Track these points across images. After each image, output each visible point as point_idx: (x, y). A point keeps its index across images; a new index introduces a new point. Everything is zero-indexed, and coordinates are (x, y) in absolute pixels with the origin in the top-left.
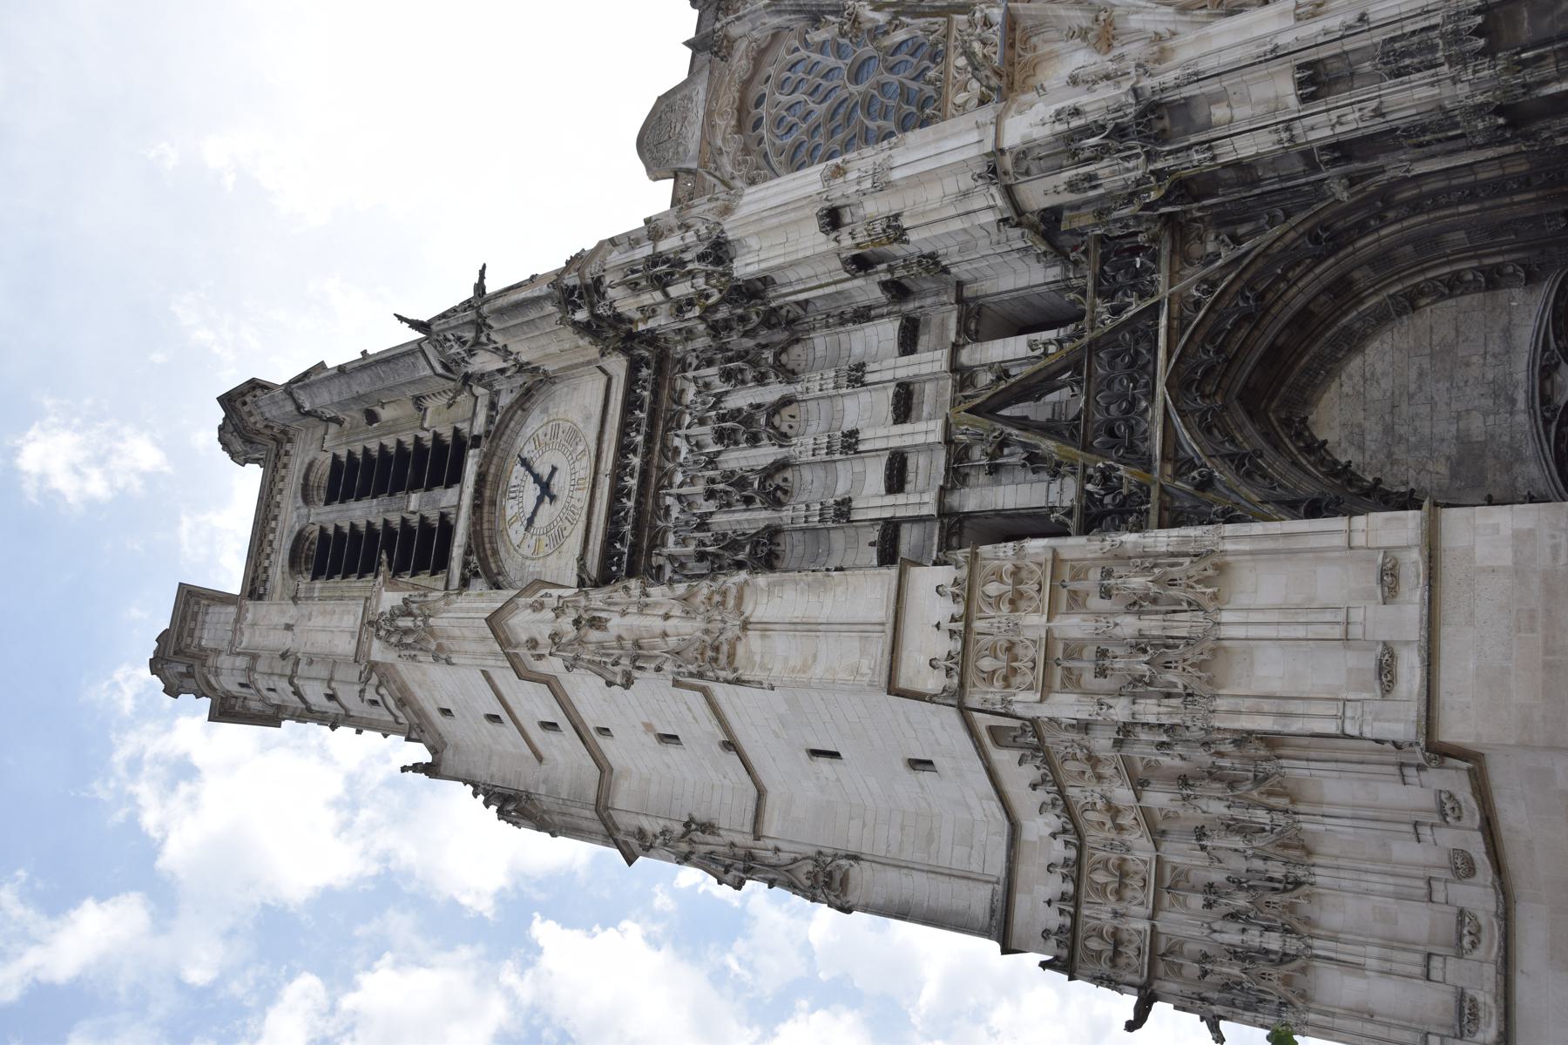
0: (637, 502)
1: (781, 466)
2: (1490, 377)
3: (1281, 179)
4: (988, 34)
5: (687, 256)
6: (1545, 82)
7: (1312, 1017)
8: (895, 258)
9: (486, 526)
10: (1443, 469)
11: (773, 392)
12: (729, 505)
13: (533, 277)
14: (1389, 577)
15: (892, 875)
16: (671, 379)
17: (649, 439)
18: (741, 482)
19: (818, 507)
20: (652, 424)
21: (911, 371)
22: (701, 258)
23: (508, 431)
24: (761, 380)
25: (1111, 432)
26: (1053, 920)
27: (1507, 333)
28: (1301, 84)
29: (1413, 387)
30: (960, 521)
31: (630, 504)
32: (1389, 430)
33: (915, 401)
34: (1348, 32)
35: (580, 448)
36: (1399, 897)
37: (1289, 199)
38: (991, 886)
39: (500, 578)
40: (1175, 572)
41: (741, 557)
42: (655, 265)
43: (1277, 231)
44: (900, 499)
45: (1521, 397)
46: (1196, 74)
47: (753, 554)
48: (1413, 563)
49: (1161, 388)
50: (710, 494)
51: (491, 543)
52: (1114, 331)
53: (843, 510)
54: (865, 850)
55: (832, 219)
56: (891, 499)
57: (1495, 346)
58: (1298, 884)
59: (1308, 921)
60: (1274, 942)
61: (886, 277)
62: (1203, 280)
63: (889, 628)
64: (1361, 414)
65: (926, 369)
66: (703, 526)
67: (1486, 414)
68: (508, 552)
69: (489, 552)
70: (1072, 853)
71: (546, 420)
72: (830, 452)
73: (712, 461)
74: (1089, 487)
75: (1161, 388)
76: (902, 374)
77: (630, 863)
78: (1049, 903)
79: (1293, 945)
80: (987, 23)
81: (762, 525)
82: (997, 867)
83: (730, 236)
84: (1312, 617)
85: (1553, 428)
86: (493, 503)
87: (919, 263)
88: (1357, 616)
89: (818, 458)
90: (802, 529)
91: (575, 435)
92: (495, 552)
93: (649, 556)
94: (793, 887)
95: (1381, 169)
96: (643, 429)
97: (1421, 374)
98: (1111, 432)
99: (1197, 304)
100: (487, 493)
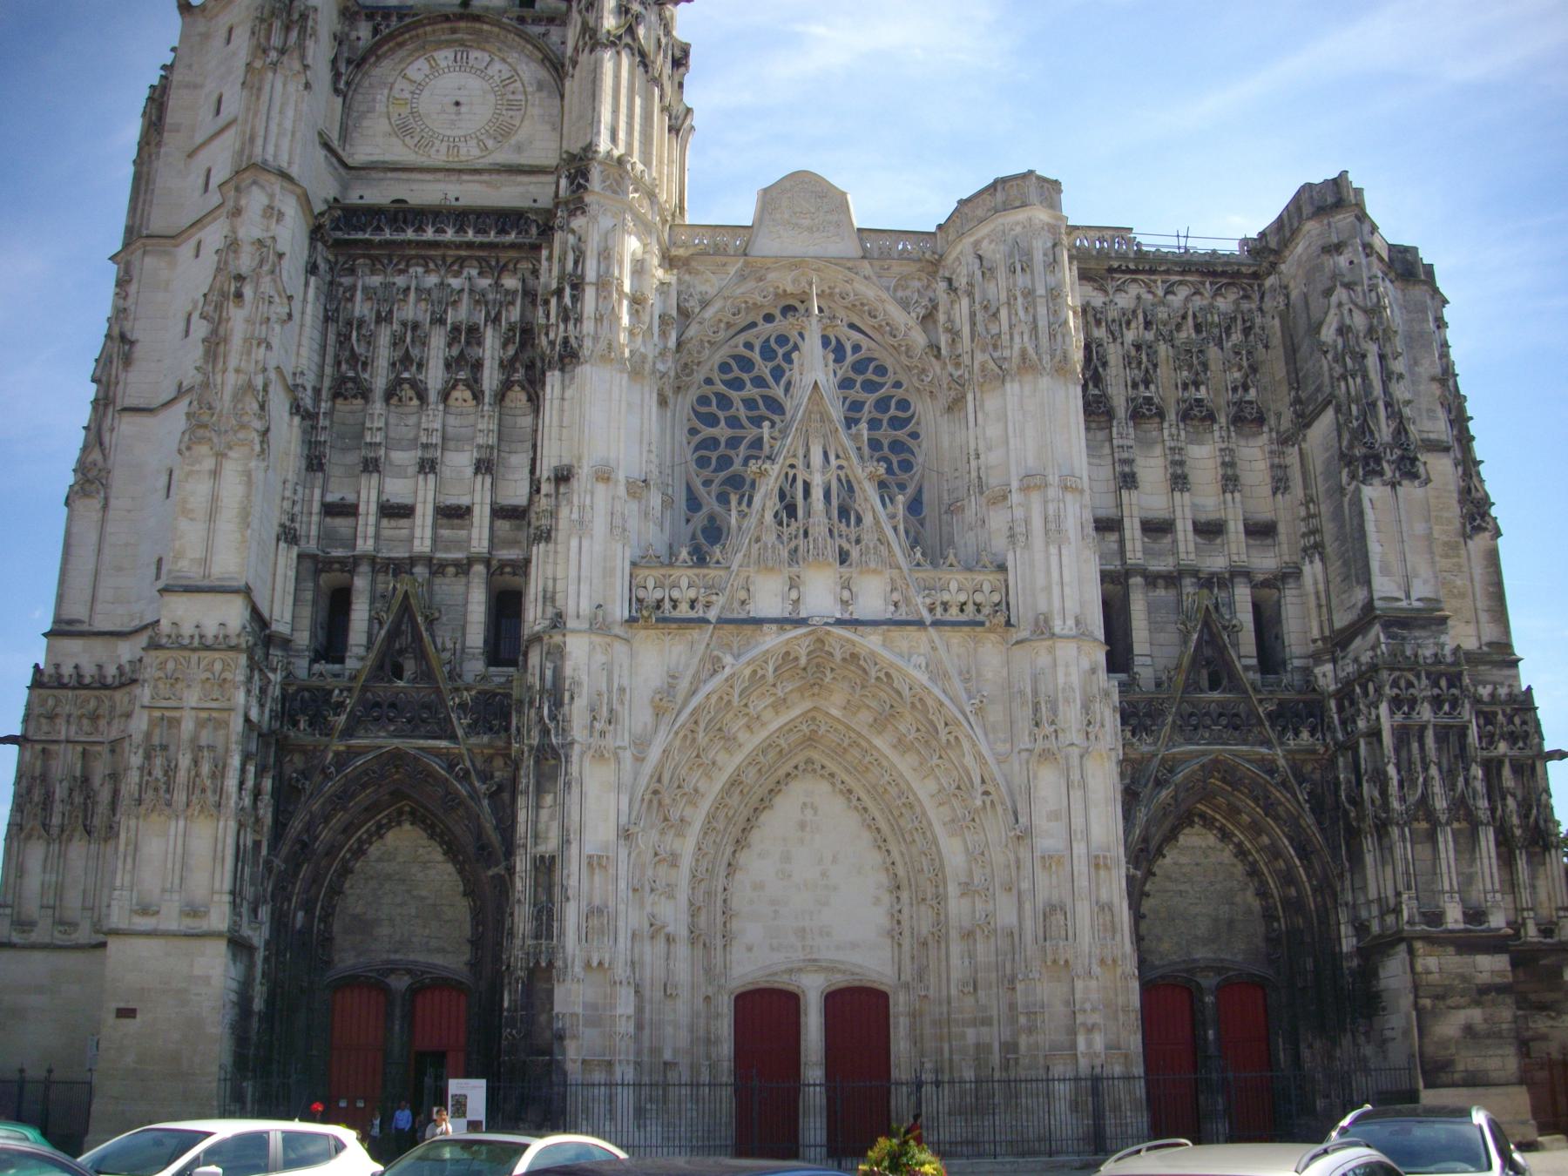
0: (410, 242)
1: (422, 396)
2: (414, 939)
5: (571, 326)
7: (16, 844)
9: (428, 29)
10: (358, 910)
11: (490, 378)
14: (193, 911)
15: (93, 537)
16: (527, 258)
17: (470, 245)
20: (482, 246)
21: (476, 520)
22: (566, 341)
23: (523, 42)
24: (501, 364)
26: (67, 670)
27: (442, 950)
28: (542, 857)
29: (415, 893)
30: (349, 571)
32: (389, 877)
33: (456, 521)
34: (564, 888)
35: (490, 143)
36: (84, 892)
38: (87, 620)
39: (373, 59)
40: (209, 793)
41: (344, 367)
42: (574, 287)
45: (398, 957)
46: (569, 788)
48: (204, 925)
49: (397, 742)
51: (411, 38)
52: (446, 707)
54: (111, 514)
55: (563, 477)
56: (373, 508)
57: (433, 943)
58: (89, 833)
59: (70, 839)
60: (56, 820)
63: (206, 583)
64: (401, 860)
65: (475, 533)
66: (379, 320)
67: (390, 936)
68: (401, 61)
69: (400, 39)
70: (109, 680)
71: (530, 89)
72: (425, 446)
73: (441, 321)
74: (337, 692)
75: (397, 742)
76: (476, 510)
77: (111, 259)
78: (76, 667)
79: (55, 831)
80: (708, 605)
82: (101, 624)
83: (578, 370)
84: (177, 873)
85: (374, 974)
86: (454, 31)
88: (176, 897)
89: (422, 433)
91: (503, 133)
92: (401, 45)
93: (364, 256)
94: (86, 449)
96: (480, 239)
97: (423, 899)
99: (451, 767)
100: (462, 24)
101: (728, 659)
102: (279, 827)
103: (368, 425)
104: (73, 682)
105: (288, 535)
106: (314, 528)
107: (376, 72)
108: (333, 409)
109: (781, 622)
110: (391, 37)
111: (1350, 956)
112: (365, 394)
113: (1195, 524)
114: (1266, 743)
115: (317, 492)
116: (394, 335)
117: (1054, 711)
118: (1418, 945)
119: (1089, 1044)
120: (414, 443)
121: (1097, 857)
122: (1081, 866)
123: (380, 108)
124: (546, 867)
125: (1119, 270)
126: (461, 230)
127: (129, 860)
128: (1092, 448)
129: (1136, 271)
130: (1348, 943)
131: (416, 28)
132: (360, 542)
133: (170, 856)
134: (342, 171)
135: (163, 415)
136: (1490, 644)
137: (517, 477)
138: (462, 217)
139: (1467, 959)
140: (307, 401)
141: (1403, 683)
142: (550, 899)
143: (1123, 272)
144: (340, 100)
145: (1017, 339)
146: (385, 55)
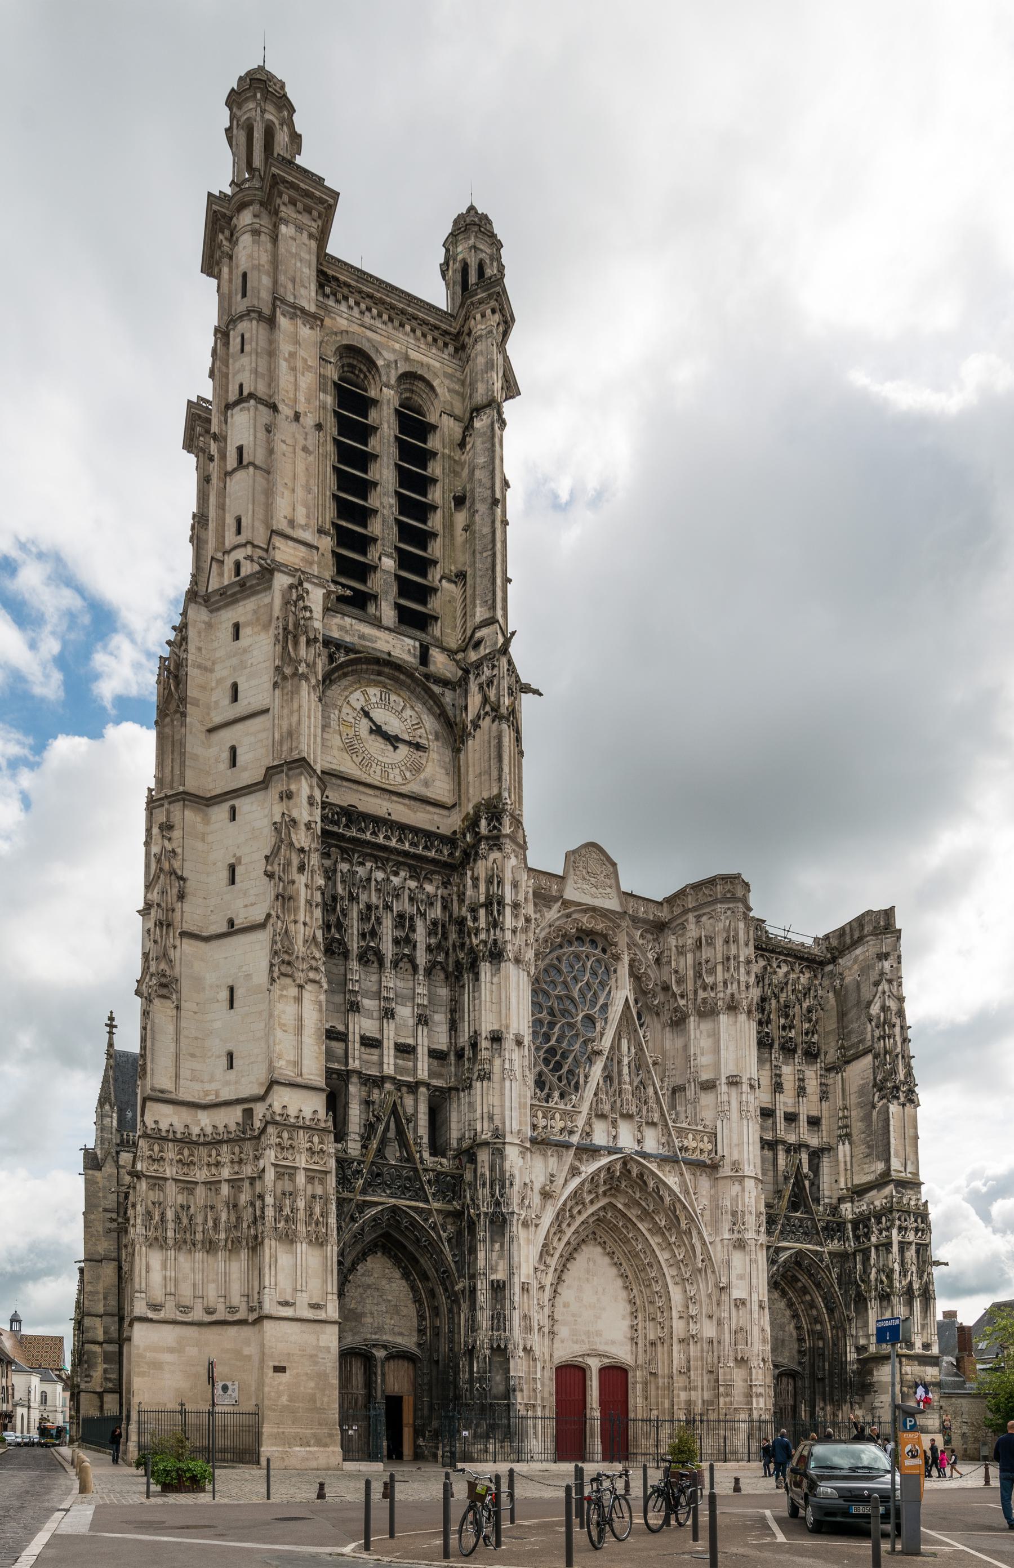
0: (369, 842)
3: (469, 1264)
4: (566, 1133)
6: (478, 1362)
8: (474, 1064)
9: (364, 667)
12: (362, 919)
13: (521, 753)
18: (373, 934)
19: (357, 989)
25: (378, 1175)
31: (368, 836)
37: (460, 1265)
41: (333, 930)
43: (450, 1258)
44: (357, 1045)
47: (333, 940)
50: (369, 907)
53: (354, 1007)
56: (357, 1038)
61: (466, 1053)
62: (435, 1224)
66: (353, 898)
68: (345, 689)
69: (346, 670)
80: (571, 1132)
81: (350, 948)
87: (468, 1078)
90: (345, 975)
93: (336, 846)
95: (464, 1302)
98: (378, 1175)
99: (426, 1220)
101: (583, 1168)
103: (349, 977)
104: (202, 1140)
109: (611, 1151)
110: (341, 666)
111: (852, 1363)
112: (346, 955)
116: (360, 912)
117: (743, 1217)
118: (904, 1359)
119: (758, 1404)
120: (378, 995)
121: (761, 1301)
122: (755, 1307)
124: (498, 1288)
126: (400, 840)
127: (273, 1268)
128: (761, 1061)
130: (852, 1356)
131: (356, 664)
133: (299, 1267)
135: (214, 944)
137: (438, 1029)
138: (403, 829)
139: (922, 1368)
141: (903, 1219)
142: (503, 1308)
145: (729, 985)
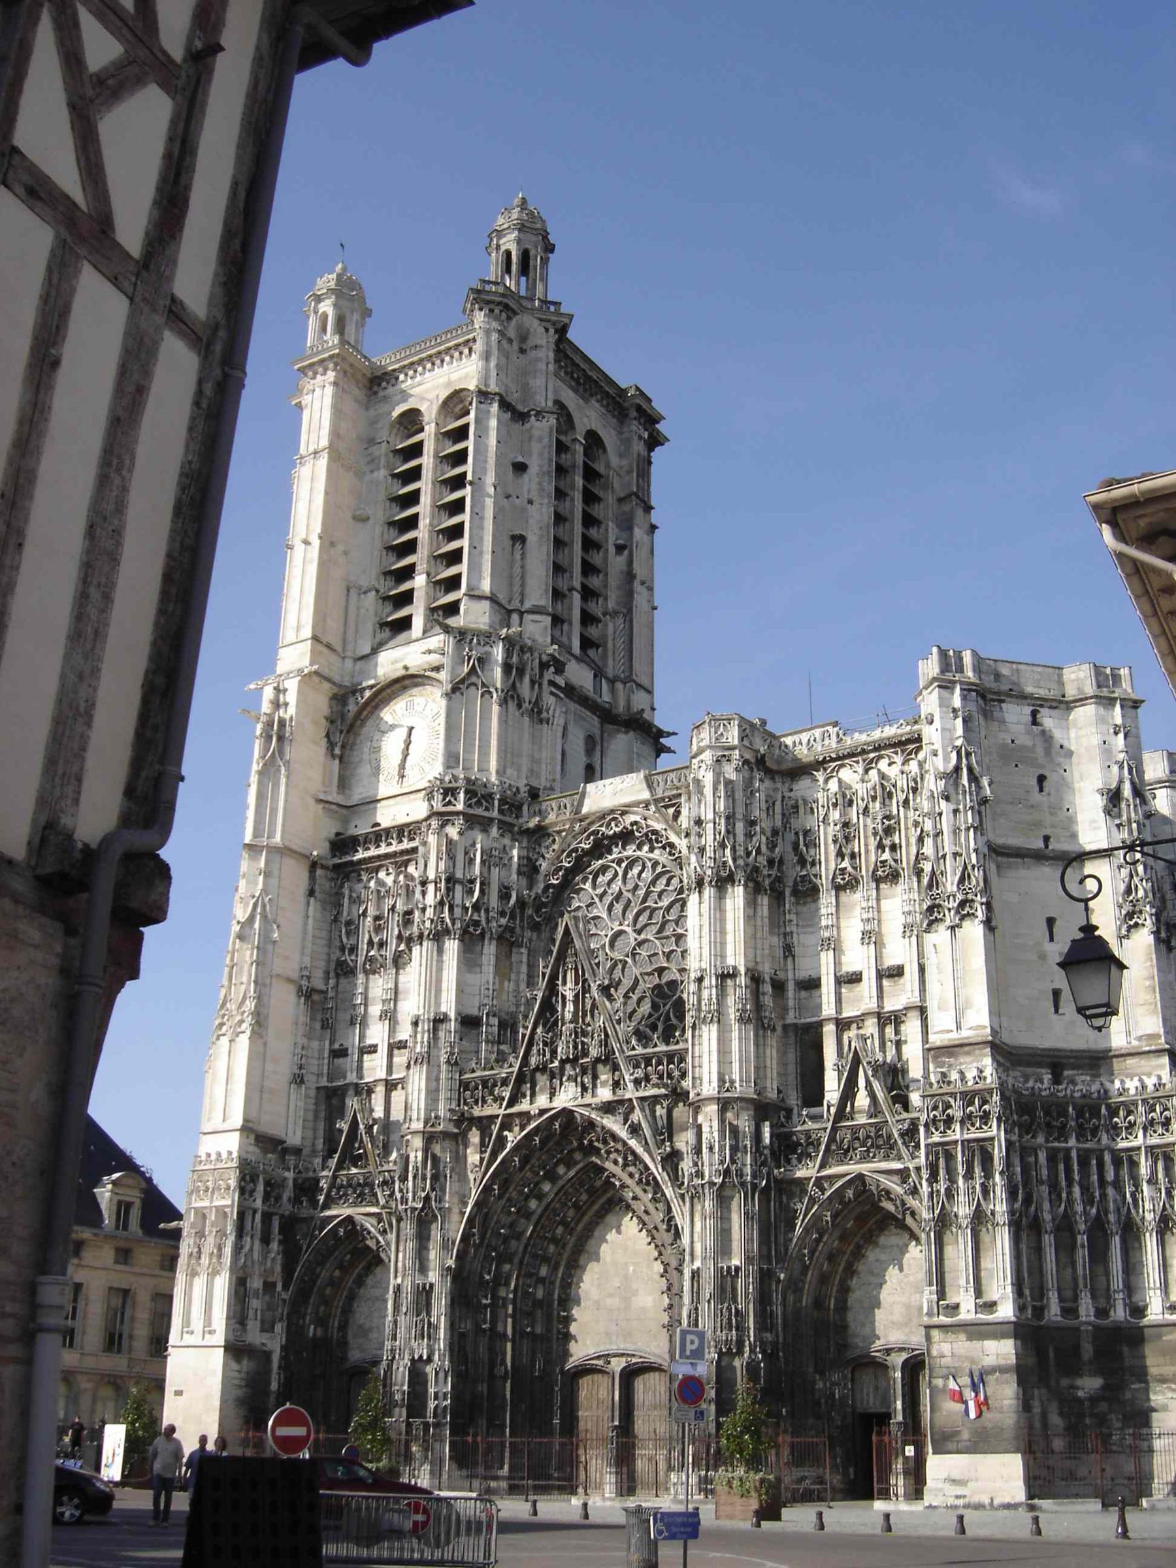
9: (389, 691)
69: (373, 704)
72: (384, 1001)
100: (407, 682)
102: (288, 1270)
105: (298, 1080)
106: (326, 1067)
107: (364, 731)
108: (337, 985)
113: (878, 971)
114: (899, 1158)
115: (327, 1042)
123: (366, 757)
125: (824, 761)
129: (839, 758)
132: (349, 1074)
134: (344, 811)
136: (1140, 1038)
139: (977, 1344)
140: (319, 984)
143: (830, 761)
144: (337, 761)
146: (367, 718)
